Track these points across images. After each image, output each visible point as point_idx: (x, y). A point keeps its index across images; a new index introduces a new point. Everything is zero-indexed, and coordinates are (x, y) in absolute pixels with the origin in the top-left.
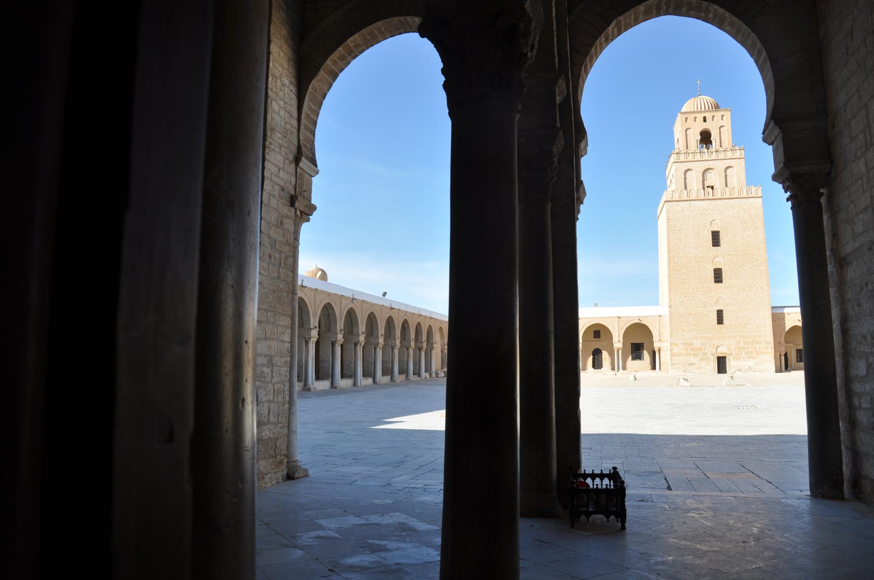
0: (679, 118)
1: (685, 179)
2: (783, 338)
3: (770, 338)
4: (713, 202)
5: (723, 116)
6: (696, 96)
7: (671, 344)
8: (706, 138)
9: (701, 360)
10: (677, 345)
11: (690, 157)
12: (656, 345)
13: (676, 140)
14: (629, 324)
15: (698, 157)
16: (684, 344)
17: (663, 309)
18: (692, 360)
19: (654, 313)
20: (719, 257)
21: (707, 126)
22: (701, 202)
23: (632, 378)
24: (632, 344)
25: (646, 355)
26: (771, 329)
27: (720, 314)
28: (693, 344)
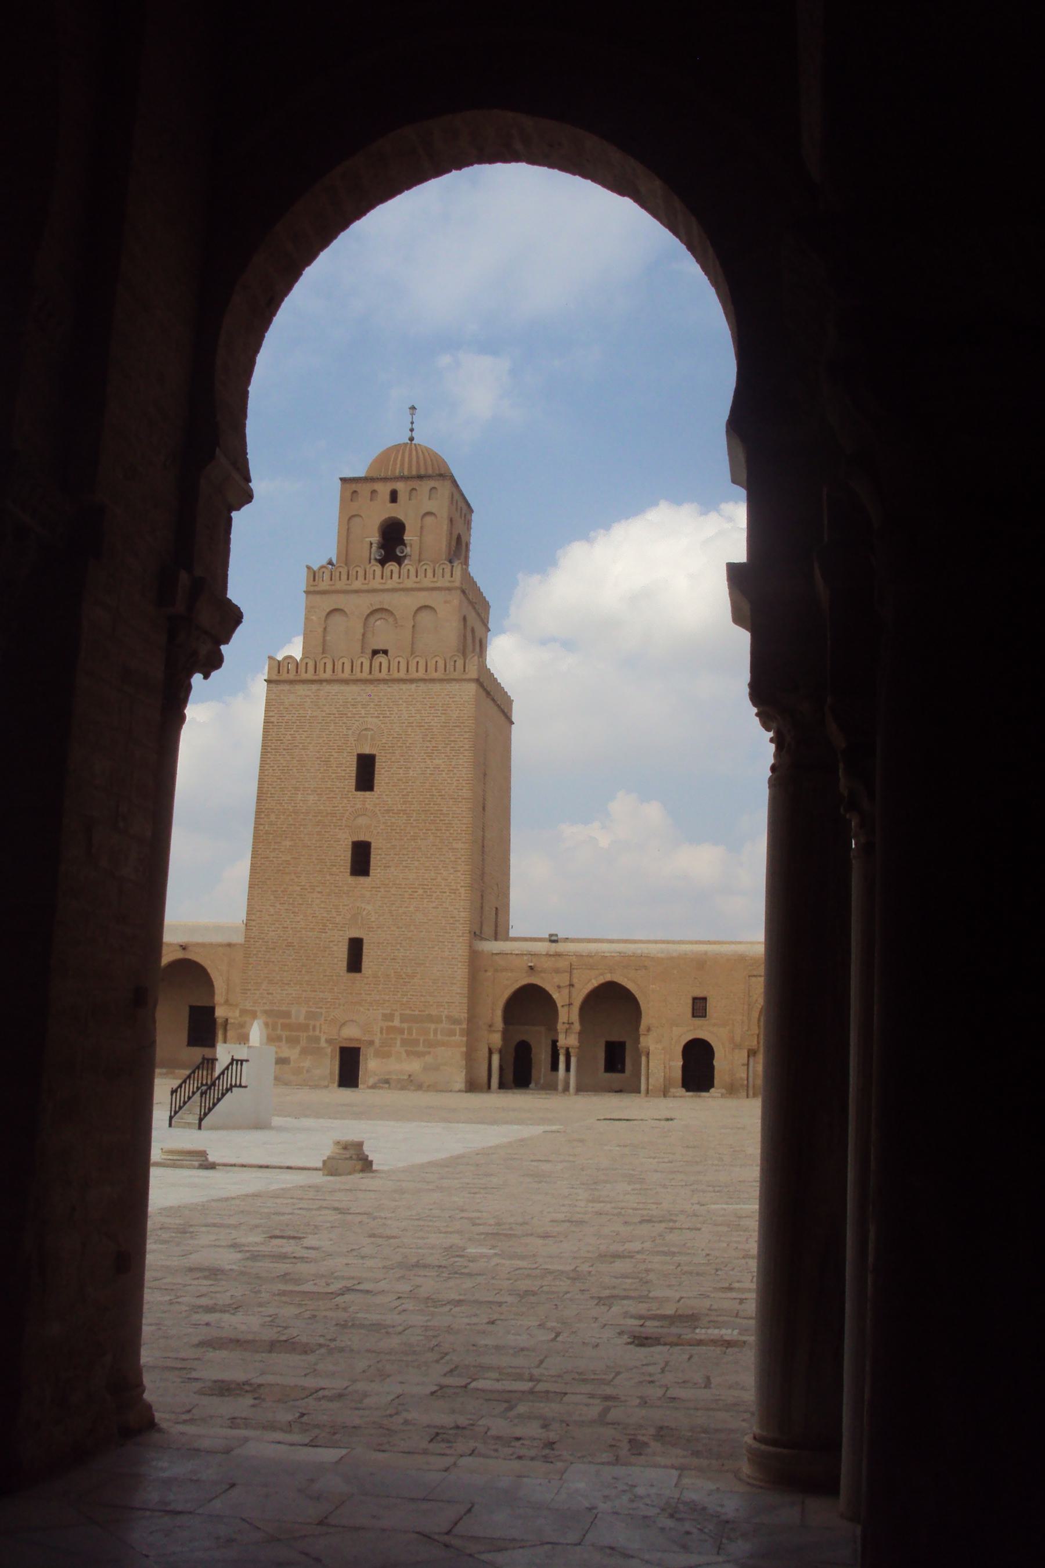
2: (499, 1013)
4: (369, 688)
9: (304, 1052)
12: (220, 1013)
21: (397, 512)
26: (465, 991)
27: (356, 947)
28: (287, 1014)
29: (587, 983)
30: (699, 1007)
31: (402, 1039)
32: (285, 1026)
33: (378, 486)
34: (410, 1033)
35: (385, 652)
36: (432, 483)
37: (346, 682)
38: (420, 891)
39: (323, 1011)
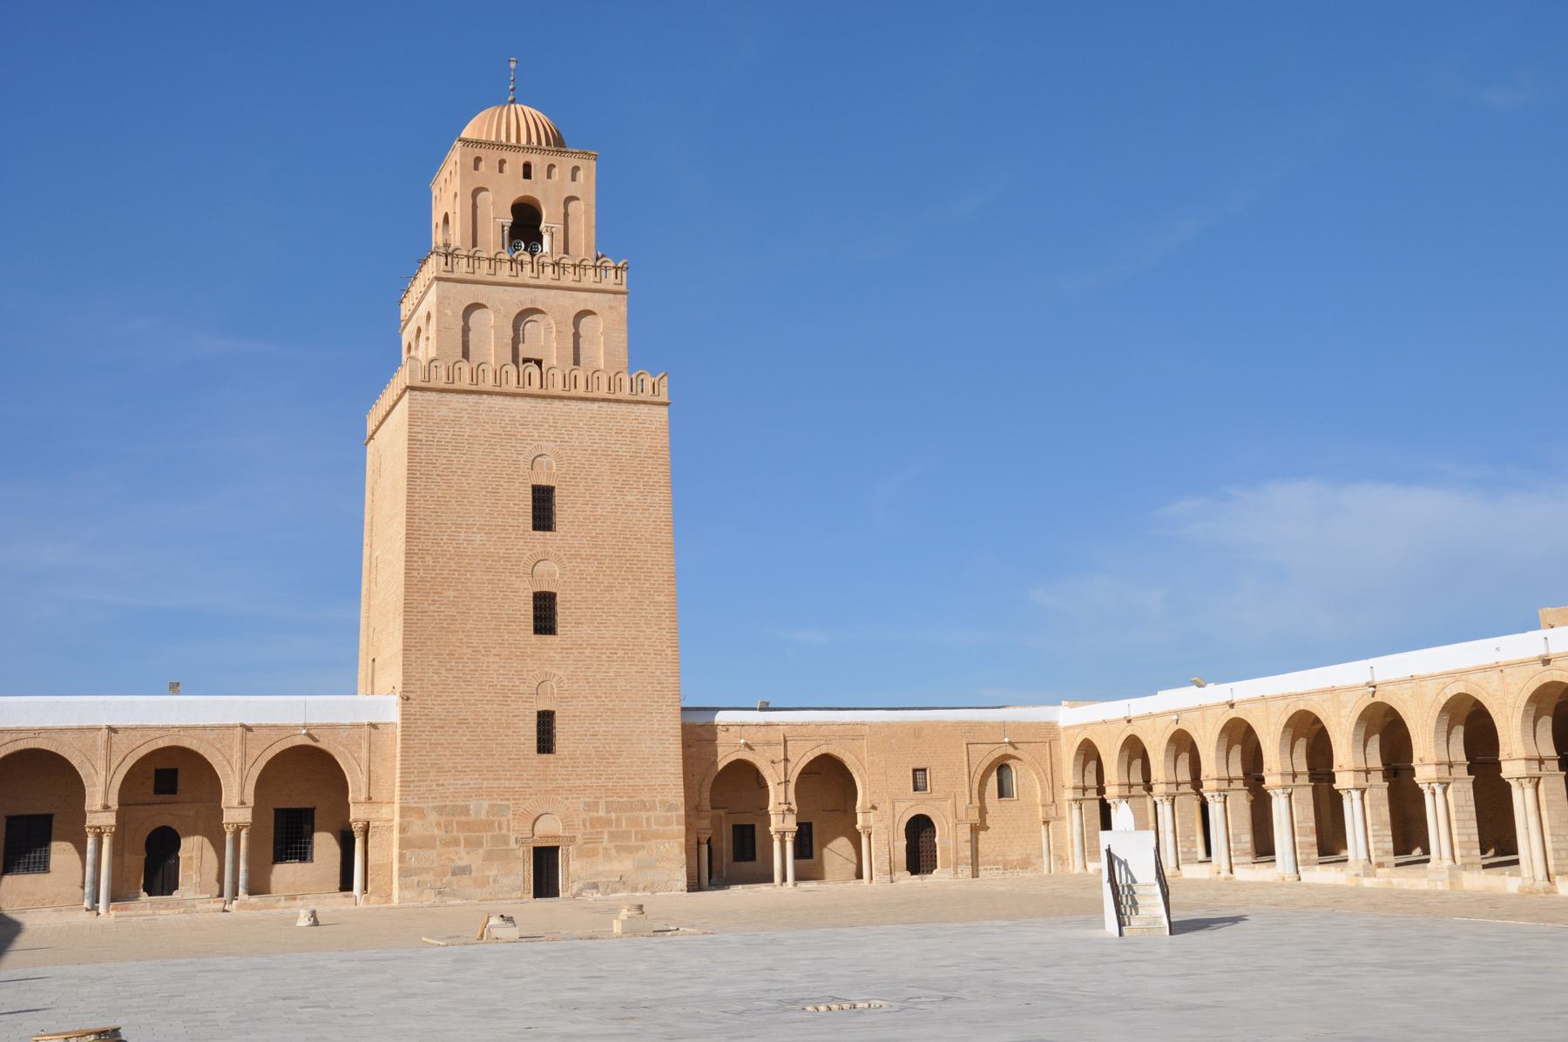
0: (456, 155)
1: (466, 330)
2: (707, 795)
3: (676, 794)
4: (541, 404)
5: (576, 169)
6: (500, 101)
7: (404, 811)
8: (525, 224)
9: (490, 857)
10: (421, 813)
11: (483, 270)
12: (357, 814)
13: (437, 218)
14: (277, 749)
15: (504, 273)
16: (440, 810)
17: (381, 703)
18: (463, 857)
19: (360, 709)
20: (551, 561)
22: (508, 401)
23: (303, 921)
24: (277, 811)
25: (325, 845)
27: (545, 722)
28: (466, 810)
29: (802, 757)
30: (919, 780)
31: (611, 834)
32: (465, 826)
33: (508, 156)
34: (619, 824)
35: (539, 363)
36: (575, 162)
37: (514, 395)
38: (620, 653)
39: (510, 803)
